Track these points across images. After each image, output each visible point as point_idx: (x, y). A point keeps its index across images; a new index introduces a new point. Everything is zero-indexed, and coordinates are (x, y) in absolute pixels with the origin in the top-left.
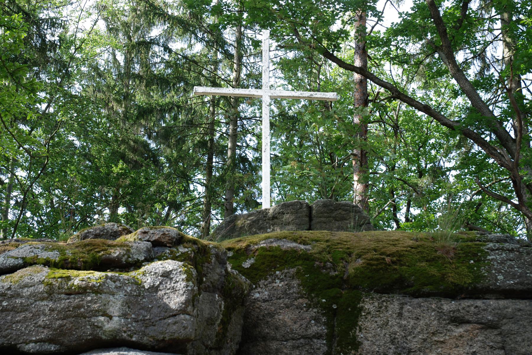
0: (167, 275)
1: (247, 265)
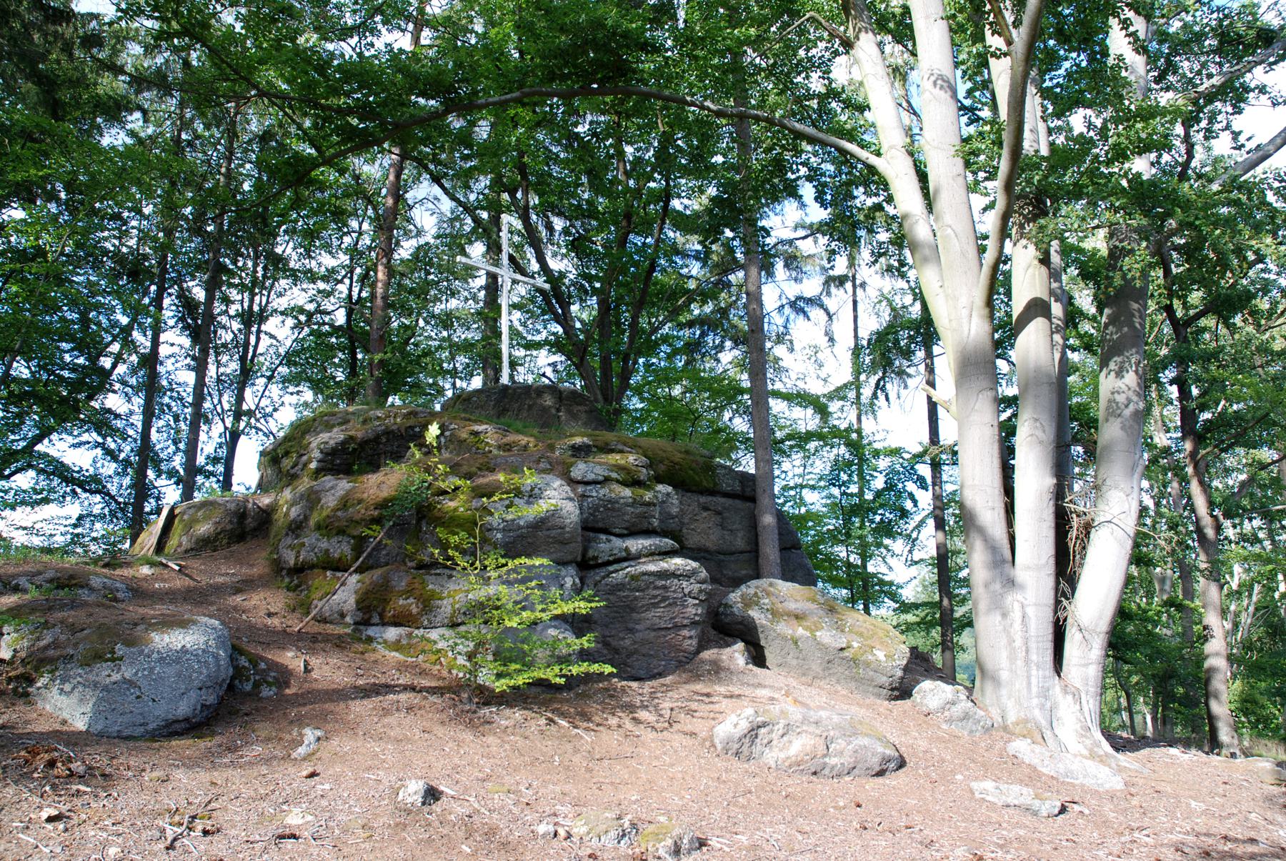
0: (668, 494)
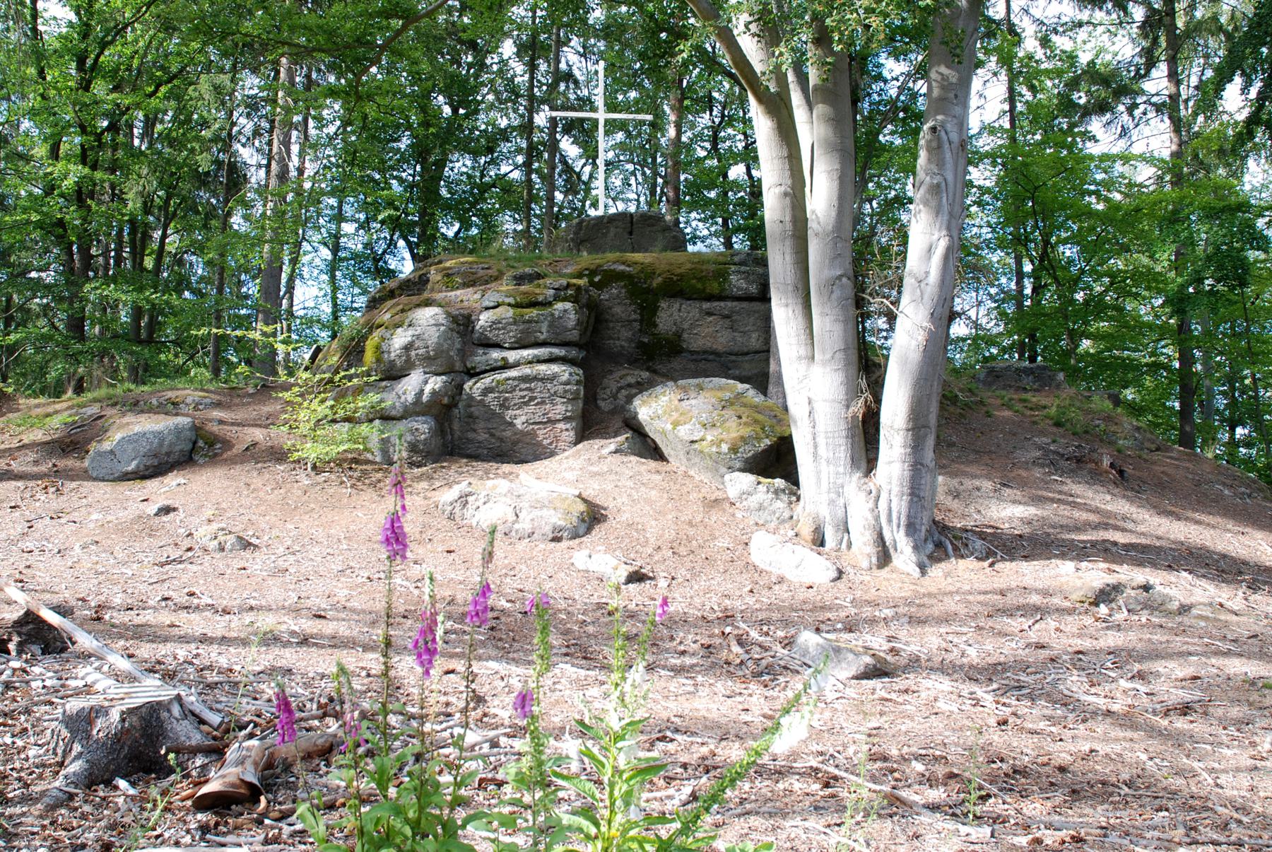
1: (597, 279)
